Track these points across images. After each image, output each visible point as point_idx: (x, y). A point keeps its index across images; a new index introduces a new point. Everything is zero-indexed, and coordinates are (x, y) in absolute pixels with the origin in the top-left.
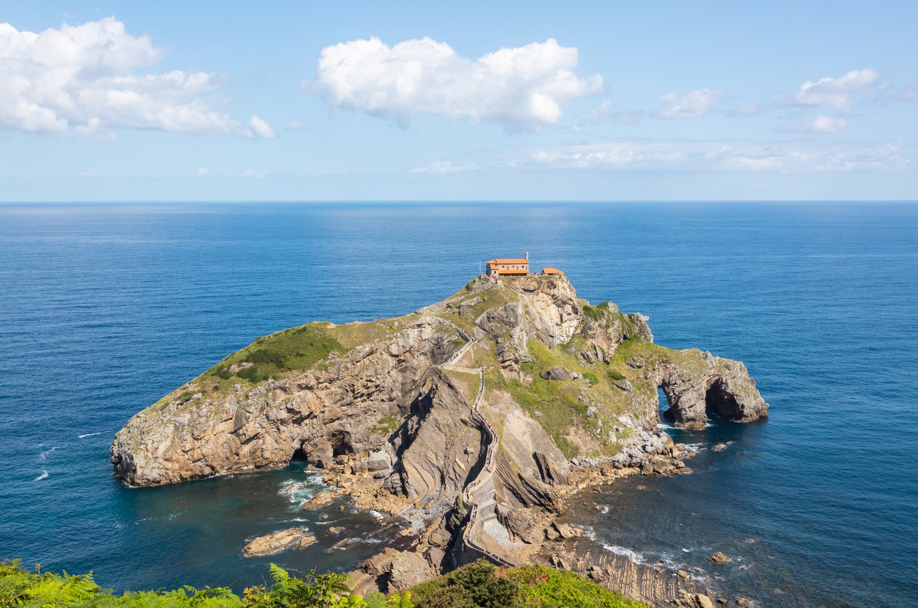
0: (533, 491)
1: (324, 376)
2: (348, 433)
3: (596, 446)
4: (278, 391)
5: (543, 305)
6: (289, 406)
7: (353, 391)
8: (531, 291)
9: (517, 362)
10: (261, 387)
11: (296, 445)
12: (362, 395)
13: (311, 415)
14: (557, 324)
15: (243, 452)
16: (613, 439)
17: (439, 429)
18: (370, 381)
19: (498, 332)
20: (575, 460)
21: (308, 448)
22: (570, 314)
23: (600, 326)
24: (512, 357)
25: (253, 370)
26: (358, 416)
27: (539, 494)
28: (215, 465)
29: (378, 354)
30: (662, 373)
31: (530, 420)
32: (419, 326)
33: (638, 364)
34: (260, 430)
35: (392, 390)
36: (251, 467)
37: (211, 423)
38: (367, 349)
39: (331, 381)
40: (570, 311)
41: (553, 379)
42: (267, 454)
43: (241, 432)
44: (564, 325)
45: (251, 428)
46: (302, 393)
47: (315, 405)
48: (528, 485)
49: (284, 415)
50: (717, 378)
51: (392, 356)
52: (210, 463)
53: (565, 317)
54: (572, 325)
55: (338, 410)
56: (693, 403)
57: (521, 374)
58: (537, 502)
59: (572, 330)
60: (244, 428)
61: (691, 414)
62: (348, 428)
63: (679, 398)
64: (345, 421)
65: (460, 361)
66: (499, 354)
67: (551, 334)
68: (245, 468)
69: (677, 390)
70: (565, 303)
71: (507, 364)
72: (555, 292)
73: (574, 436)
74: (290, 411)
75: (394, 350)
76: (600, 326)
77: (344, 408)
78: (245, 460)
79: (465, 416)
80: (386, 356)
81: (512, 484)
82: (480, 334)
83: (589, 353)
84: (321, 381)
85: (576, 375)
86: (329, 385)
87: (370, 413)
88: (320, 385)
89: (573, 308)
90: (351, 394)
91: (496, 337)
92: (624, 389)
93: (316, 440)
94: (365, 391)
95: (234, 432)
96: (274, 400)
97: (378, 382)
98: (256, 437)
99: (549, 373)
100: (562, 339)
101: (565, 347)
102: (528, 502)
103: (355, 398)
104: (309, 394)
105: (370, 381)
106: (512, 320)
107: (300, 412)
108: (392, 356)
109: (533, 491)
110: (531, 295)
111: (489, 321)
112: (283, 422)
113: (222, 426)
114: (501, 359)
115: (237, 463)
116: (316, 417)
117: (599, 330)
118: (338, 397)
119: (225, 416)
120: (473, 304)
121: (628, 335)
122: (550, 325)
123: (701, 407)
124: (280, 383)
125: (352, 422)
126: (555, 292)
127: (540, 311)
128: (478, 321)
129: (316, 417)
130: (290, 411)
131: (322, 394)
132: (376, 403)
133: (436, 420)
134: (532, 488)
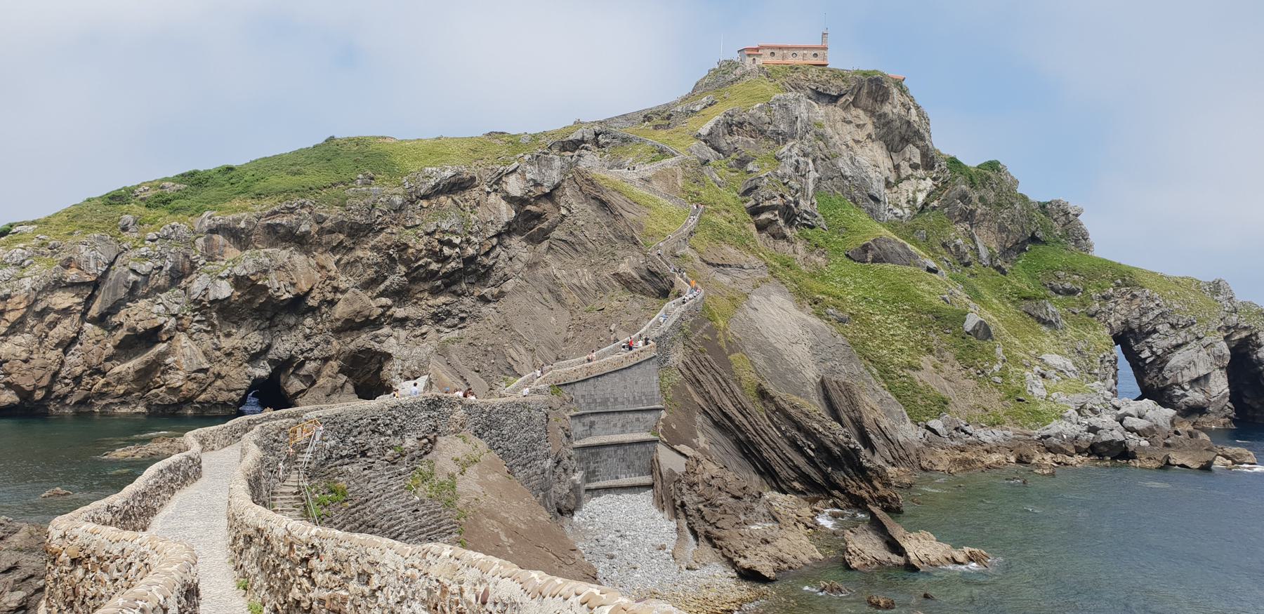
0: (801, 439)
1: (334, 214)
2: (388, 357)
3: (994, 401)
4: (219, 239)
5: (861, 135)
6: (238, 270)
7: (407, 263)
8: (833, 99)
9: (790, 221)
10: (182, 225)
11: (262, 371)
12: (433, 275)
13: (298, 306)
15: (117, 369)
17: (559, 300)
18: (451, 244)
19: (751, 152)
20: (936, 424)
21: (294, 385)
22: (915, 167)
23: (981, 199)
24: (778, 201)
26: (420, 323)
27: (822, 448)
28: (26, 383)
29: (475, 193)
30: (1122, 307)
31: (815, 321)
32: (576, 145)
33: (1068, 285)
34: (161, 320)
35: (506, 278)
36: (141, 409)
37: (27, 283)
38: (448, 173)
39: (358, 232)
40: (917, 160)
41: (876, 260)
42: (176, 379)
43: (115, 320)
44: (904, 186)
45: (140, 314)
46: (282, 254)
47: (309, 280)
48: (789, 417)
49: (224, 290)
50: (1244, 334)
51: (510, 199)
52: (15, 378)
53: (906, 170)
54: (921, 187)
55: (373, 304)
56: (1202, 372)
57: (800, 246)
58: (817, 477)
59: (921, 198)
60: (123, 312)
61: (1195, 396)
62: (390, 346)
63: (1160, 361)
64: (386, 330)
66: (747, 192)
67: (872, 192)
68: (124, 410)
69: (1159, 343)
70: (905, 140)
71: (763, 217)
72: (887, 108)
74: (238, 282)
75: (514, 186)
76: (981, 199)
77: (385, 301)
78: (121, 389)
79: (624, 268)
80: (493, 198)
81: (731, 409)
82: (709, 153)
83: (959, 241)
84: (327, 224)
86: (348, 243)
87: (450, 321)
88: (326, 238)
89: (924, 155)
90: (402, 269)
91: (742, 163)
92: (1039, 319)
93: (310, 367)
94: (434, 266)
95: (101, 320)
96: (211, 259)
97: (470, 251)
98: (152, 336)
99: (865, 248)
100: (900, 212)
102: (784, 472)
103: (413, 281)
104: (299, 259)
105: (451, 244)
106: (783, 127)
107: (265, 288)
108: (510, 199)
109: (801, 439)
110: (831, 107)
111: (731, 133)
112: (227, 312)
113: (63, 300)
114: (752, 202)
115: (101, 395)
116: (313, 310)
118: (371, 273)
119: (72, 275)
120: (698, 108)
121: (1040, 234)
122: (873, 175)
123: (1220, 385)
124: (220, 218)
125: (403, 333)
126: (887, 108)
127: (851, 143)
128: (704, 130)
129: (313, 310)
130: (238, 282)
131: (330, 260)
132: (467, 301)
133: (554, 279)
134: (800, 428)
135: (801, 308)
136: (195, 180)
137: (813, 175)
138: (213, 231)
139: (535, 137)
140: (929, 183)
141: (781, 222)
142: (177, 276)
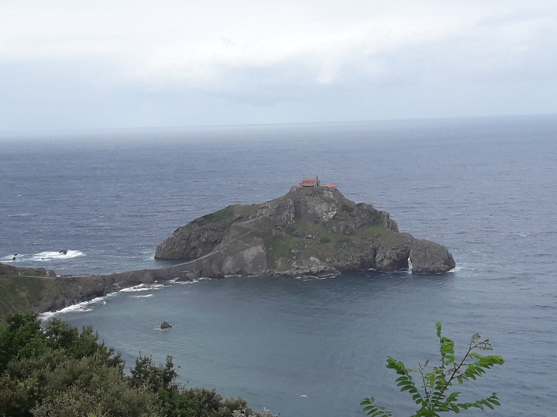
14: (326, 212)
16: (294, 264)
23: (350, 215)
25: (202, 221)
31: (262, 251)
45: (194, 244)
53: (331, 209)
65: (251, 223)
73: (279, 263)
76: (350, 215)
85: (310, 236)
101: (325, 224)
113: (183, 242)
117: (349, 217)
119: (184, 238)
127: (314, 204)
135: (263, 249)
136: (205, 217)
137: (292, 216)
138: (203, 230)
139: (258, 205)
140: (335, 212)
141: (281, 228)
142: (199, 237)
